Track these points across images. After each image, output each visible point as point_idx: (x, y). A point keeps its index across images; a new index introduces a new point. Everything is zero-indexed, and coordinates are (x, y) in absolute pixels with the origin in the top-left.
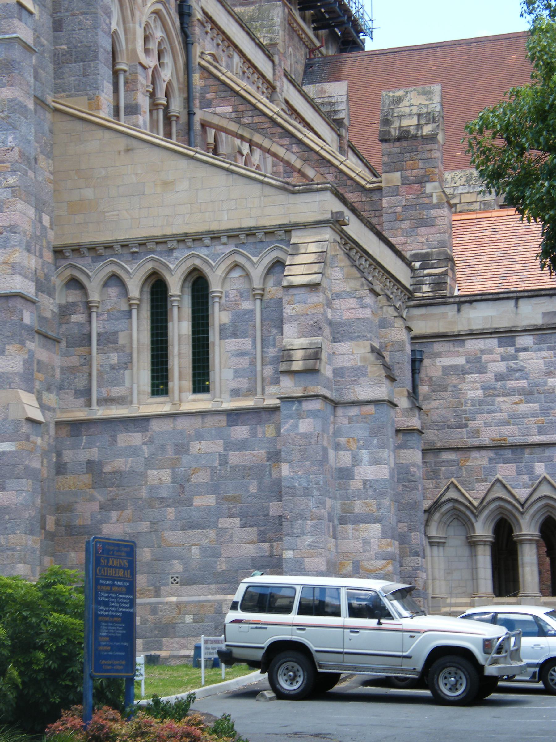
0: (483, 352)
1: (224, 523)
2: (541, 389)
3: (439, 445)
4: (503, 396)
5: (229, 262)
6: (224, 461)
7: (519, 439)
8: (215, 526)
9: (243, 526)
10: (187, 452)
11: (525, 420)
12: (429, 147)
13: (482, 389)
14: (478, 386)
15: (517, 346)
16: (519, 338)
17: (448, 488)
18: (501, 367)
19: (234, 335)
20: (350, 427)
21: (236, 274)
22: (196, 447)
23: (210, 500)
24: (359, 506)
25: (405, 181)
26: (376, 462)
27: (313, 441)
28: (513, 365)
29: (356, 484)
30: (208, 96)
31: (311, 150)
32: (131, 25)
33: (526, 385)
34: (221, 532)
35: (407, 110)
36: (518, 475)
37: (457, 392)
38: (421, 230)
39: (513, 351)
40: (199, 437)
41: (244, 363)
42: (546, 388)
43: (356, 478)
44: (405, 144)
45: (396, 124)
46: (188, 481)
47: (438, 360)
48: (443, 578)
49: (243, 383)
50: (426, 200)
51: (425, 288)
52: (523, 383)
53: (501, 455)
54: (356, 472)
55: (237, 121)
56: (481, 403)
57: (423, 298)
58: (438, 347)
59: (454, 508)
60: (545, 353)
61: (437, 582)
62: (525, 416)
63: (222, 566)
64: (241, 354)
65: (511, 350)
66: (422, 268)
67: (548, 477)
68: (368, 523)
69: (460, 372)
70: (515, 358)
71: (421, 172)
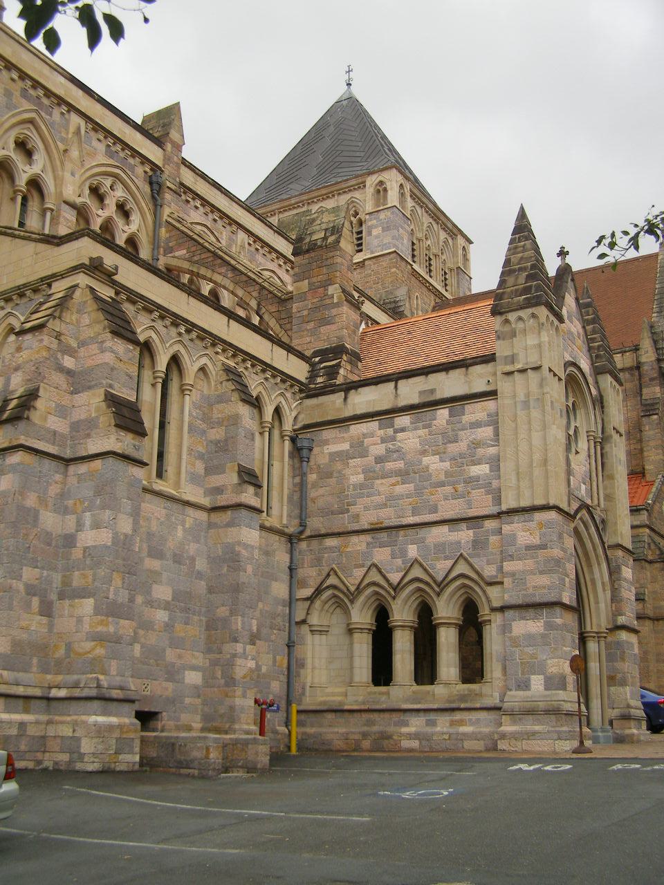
0: (365, 436)
2: (416, 468)
3: (323, 531)
4: (382, 478)
7: (395, 522)
11: (400, 502)
12: (331, 255)
13: (363, 473)
14: (360, 470)
15: (396, 427)
16: (396, 419)
17: (328, 575)
18: (379, 450)
20: (78, 487)
24: (77, 580)
25: (312, 288)
26: (96, 526)
27: (10, 500)
28: (391, 446)
29: (77, 553)
30: (171, 244)
31: (242, 273)
32: (60, 173)
33: (402, 466)
35: (318, 228)
36: (392, 558)
37: (342, 477)
38: (323, 329)
39: (392, 433)
42: (421, 467)
43: (78, 545)
44: (313, 254)
45: (307, 240)
47: (325, 447)
48: (325, 667)
50: (328, 301)
51: (320, 380)
52: (400, 465)
53: (378, 539)
54: (79, 537)
55: (189, 260)
56: (362, 486)
57: (315, 389)
58: (327, 434)
59: (335, 596)
60: (421, 432)
61: (317, 672)
62: (400, 497)
65: (390, 431)
66: (321, 362)
67: (419, 558)
68: (84, 597)
69: (344, 457)
70: (393, 439)
71: (325, 277)
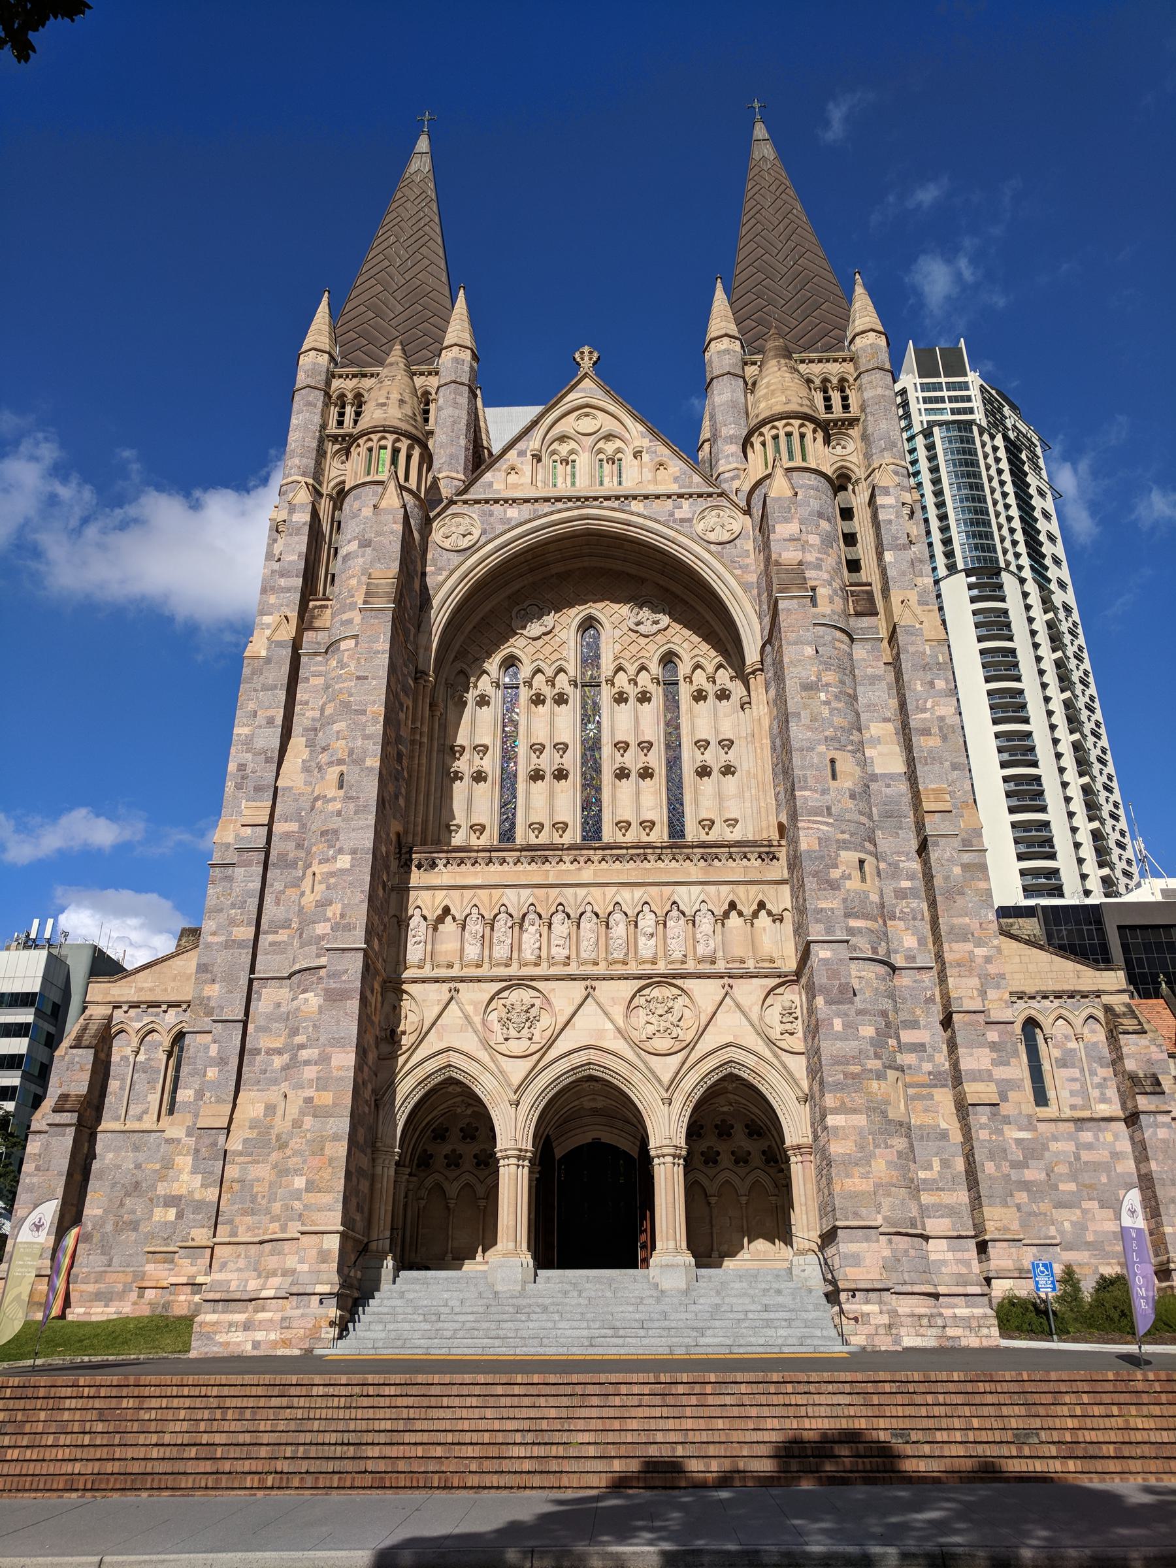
1: (1086, 1204)
5: (1055, 1014)
6: (1078, 1157)
8: (1080, 1207)
9: (1102, 1207)
10: (1048, 1149)
19: (1065, 1066)
21: (1061, 1021)
22: (1054, 1146)
23: (1072, 1187)
34: (1085, 1212)
40: (1055, 1139)
41: (1077, 1086)
46: (1053, 1171)
49: (1078, 1101)
63: (1090, 1237)
64: (1074, 1080)
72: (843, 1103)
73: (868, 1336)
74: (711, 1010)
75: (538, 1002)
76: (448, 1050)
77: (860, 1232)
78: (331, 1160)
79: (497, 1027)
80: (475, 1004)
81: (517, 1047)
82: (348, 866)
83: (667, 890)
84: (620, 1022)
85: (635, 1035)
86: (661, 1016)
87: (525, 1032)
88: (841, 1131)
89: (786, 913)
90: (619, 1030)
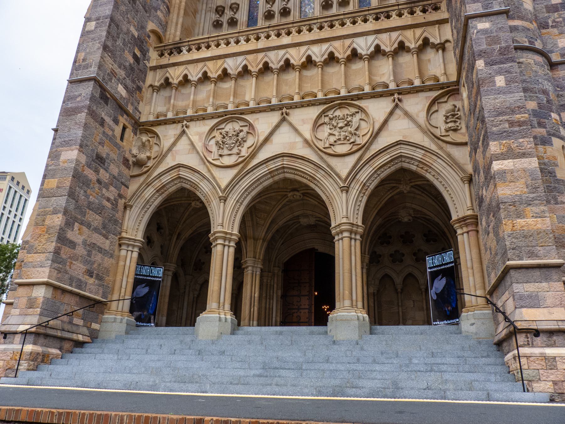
72: (510, 149)
73: (555, 383)
74: (382, 119)
75: (246, 129)
76: (179, 166)
77: (537, 273)
78: (49, 228)
79: (214, 149)
80: (200, 135)
81: (227, 161)
82: (93, 28)
83: (348, 42)
84: (308, 135)
85: (321, 145)
86: (341, 128)
87: (235, 150)
88: (509, 177)
89: (447, 45)
90: (306, 141)
